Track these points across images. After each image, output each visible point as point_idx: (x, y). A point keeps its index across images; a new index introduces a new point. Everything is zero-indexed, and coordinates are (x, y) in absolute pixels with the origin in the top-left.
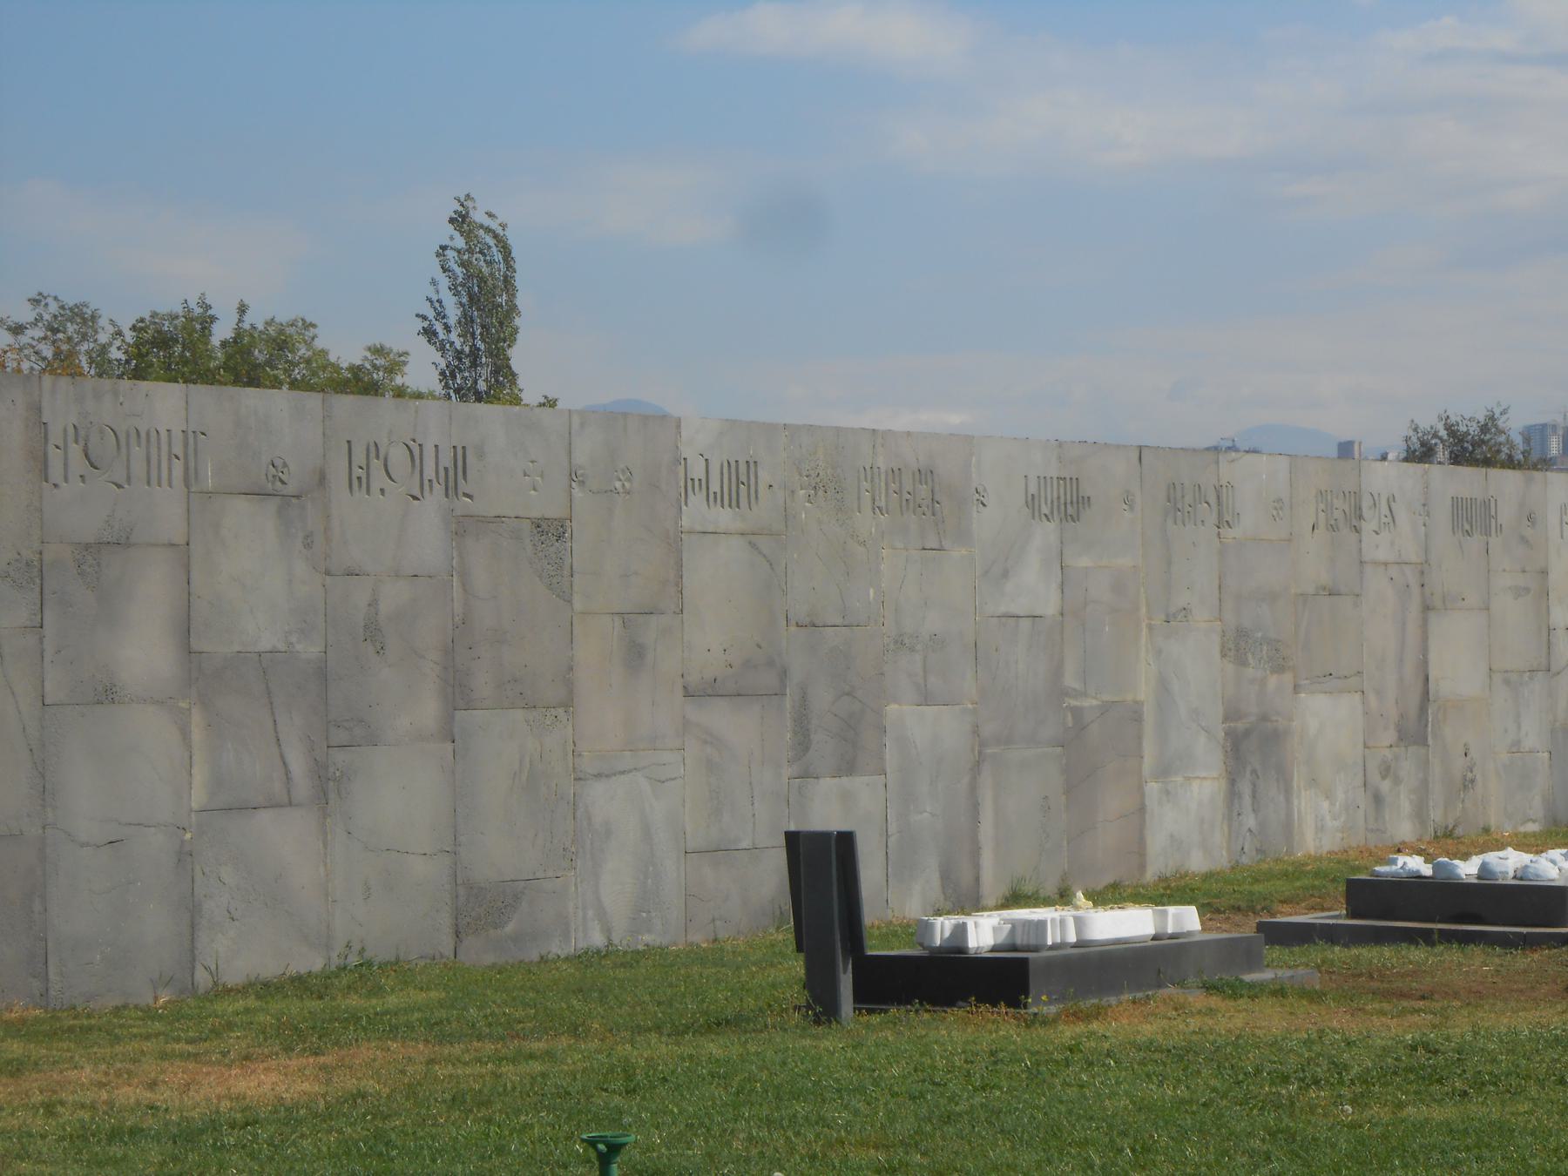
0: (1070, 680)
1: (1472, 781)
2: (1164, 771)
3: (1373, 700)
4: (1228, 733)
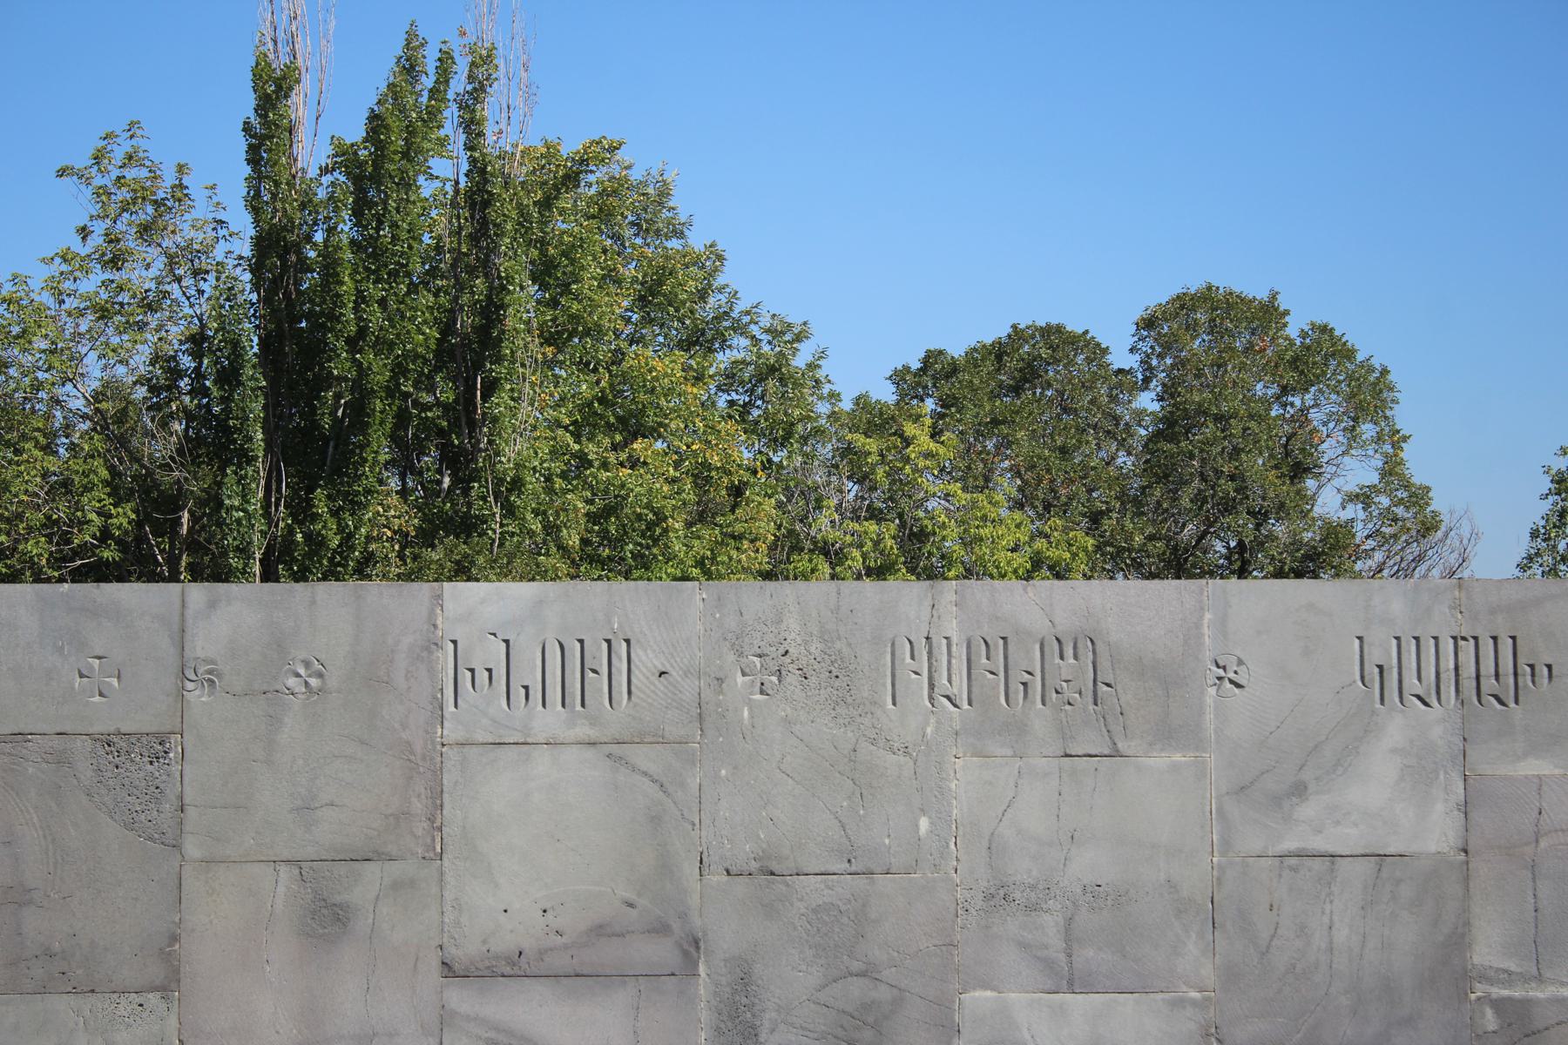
0: (1487, 951)
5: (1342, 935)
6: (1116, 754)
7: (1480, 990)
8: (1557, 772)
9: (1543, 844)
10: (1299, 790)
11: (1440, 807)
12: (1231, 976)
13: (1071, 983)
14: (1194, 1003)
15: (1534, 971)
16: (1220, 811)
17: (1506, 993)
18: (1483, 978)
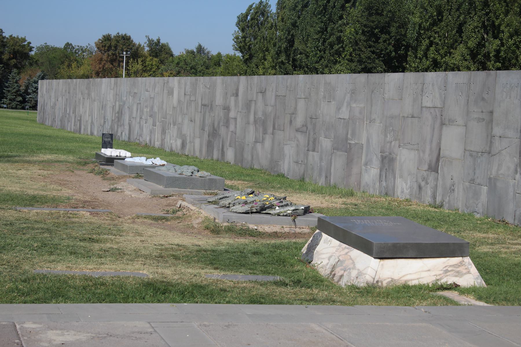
0: (349, 136)
1: (453, 190)
2: (366, 164)
3: (422, 155)
4: (382, 156)
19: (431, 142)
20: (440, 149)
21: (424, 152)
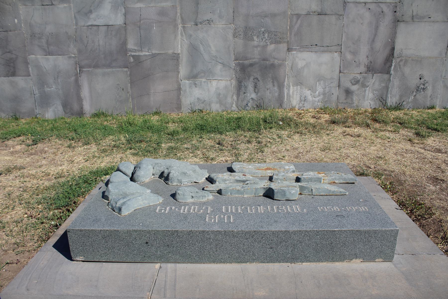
0: (131, 45)
3: (349, 57)
5: (101, 43)
6: (52, 5)
7: (130, 53)
8: (144, 6)
9: (142, 22)
10: (91, 12)
11: (119, 15)
12: (80, 51)
13: (49, 53)
14: (73, 57)
15: (140, 49)
16: (75, 17)
17: (135, 54)
18: (130, 51)
19: (373, 41)
20: (393, 49)
21: (354, 53)
